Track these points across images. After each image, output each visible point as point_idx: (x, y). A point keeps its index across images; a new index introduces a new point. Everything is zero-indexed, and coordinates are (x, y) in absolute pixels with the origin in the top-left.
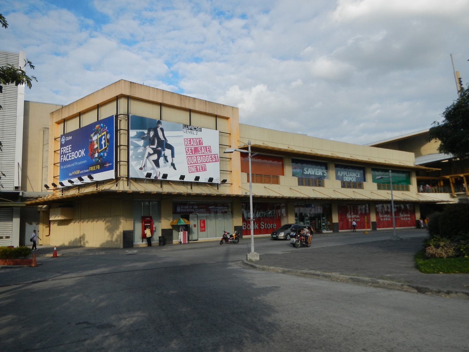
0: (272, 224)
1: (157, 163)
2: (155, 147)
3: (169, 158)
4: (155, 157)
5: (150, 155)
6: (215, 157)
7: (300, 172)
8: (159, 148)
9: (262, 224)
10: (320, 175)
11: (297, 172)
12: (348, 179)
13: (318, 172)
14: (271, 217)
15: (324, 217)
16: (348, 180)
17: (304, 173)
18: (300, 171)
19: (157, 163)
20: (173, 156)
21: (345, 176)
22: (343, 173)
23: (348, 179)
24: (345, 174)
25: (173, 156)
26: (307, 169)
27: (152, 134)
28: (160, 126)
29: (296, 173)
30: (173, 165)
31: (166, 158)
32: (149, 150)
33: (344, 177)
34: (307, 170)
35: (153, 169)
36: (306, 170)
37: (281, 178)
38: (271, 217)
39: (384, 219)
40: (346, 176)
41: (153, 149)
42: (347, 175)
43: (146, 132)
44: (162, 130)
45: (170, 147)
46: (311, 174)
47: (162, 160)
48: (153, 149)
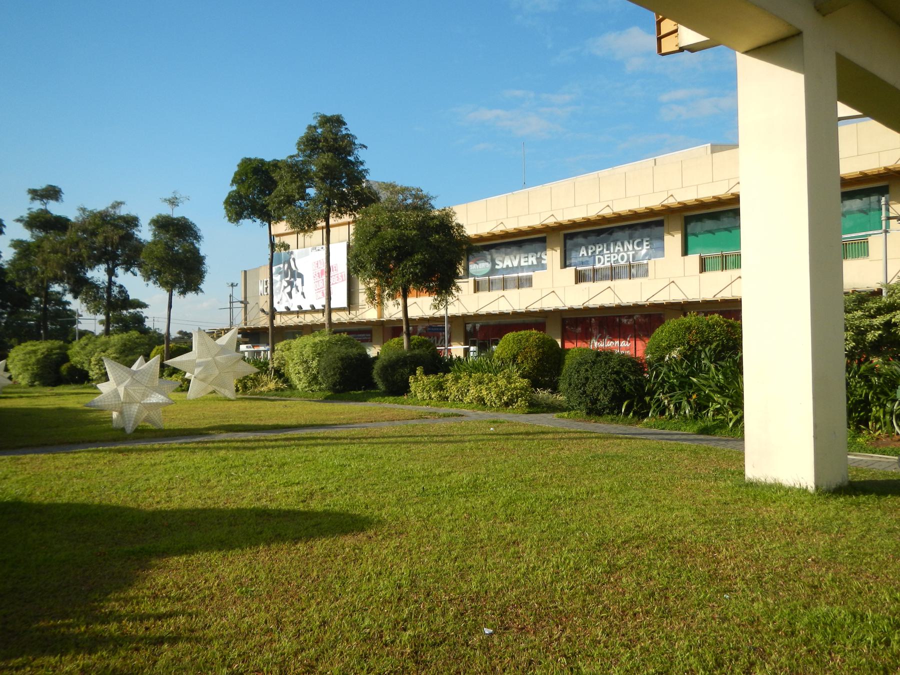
1: (290, 294)
2: (288, 279)
3: (300, 288)
4: (288, 289)
5: (285, 288)
6: (342, 276)
8: (292, 279)
10: (530, 263)
16: (608, 261)
17: (497, 267)
19: (290, 294)
20: (303, 285)
22: (594, 247)
24: (601, 249)
25: (303, 285)
26: (501, 259)
27: (286, 266)
28: (292, 256)
30: (303, 294)
31: (297, 287)
32: (286, 284)
33: (597, 257)
35: (287, 301)
41: (287, 281)
43: (281, 266)
44: (294, 260)
45: (300, 276)
47: (294, 289)
48: (287, 281)
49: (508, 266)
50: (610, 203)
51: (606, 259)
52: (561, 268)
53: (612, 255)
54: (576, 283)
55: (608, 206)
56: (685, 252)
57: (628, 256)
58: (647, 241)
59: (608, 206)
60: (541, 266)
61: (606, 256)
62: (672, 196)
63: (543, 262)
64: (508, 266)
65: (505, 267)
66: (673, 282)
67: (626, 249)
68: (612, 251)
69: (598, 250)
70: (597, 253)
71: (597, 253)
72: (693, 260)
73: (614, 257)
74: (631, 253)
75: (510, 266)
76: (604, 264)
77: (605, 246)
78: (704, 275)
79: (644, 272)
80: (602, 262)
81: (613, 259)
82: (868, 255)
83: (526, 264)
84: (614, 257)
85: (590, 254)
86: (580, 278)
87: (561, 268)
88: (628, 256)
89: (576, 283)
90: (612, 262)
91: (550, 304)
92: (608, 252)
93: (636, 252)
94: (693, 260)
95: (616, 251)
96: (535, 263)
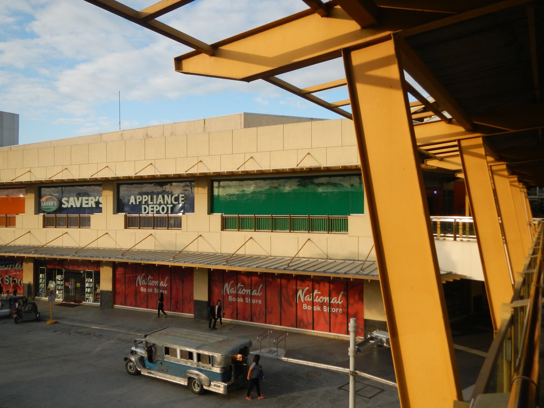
0: (20, 280)
7: (54, 206)
9: (7, 278)
10: (90, 206)
11: (48, 206)
12: (152, 209)
13: (87, 202)
14: (19, 269)
15: (91, 278)
17: (63, 206)
18: (54, 204)
21: (146, 203)
23: (152, 209)
26: (66, 199)
29: (48, 207)
33: (143, 206)
34: (68, 202)
36: (66, 201)
37: (19, 218)
38: (19, 269)
39: (241, 300)
40: (148, 205)
42: (150, 202)
46: (75, 207)
49: (72, 206)
50: (153, 162)
51: (151, 209)
52: (114, 213)
53: (155, 206)
54: (126, 227)
55: (151, 164)
56: (211, 210)
57: (168, 208)
58: (182, 197)
59: (151, 164)
60: (98, 208)
61: (150, 206)
62: (201, 161)
63: (100, 206)
64: (72, 206)
65: (69, 206)
66: (201, 236)
67: (165, 203)
68: (155, 203)
69: (144, 200)
70: (143, 203)
71: (143, 203)
72: (217, 217)
73: (157, 208)
74: (170, 206)
75: (74, 206)
76: (148, 213)
77: (149, 196)
78: (225, 233)
79: (178, 224)
80: (147, 212)
81: (155, 210)
82: (347, 231)
83: (86, 206)
84: (157, 208)
85: (137, 203)
86: (129, 223)
87: (114, 213)
88: (168, 208)
89: (126, 228)
90: (155, 212)
91: (106, 243)
92: (152, 203)
93: (174, 206)
94: (217, 217)
95: (158, 203)
96: (94, 206)
